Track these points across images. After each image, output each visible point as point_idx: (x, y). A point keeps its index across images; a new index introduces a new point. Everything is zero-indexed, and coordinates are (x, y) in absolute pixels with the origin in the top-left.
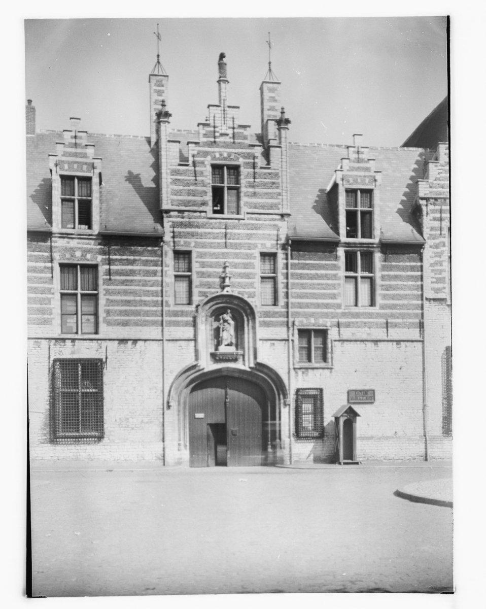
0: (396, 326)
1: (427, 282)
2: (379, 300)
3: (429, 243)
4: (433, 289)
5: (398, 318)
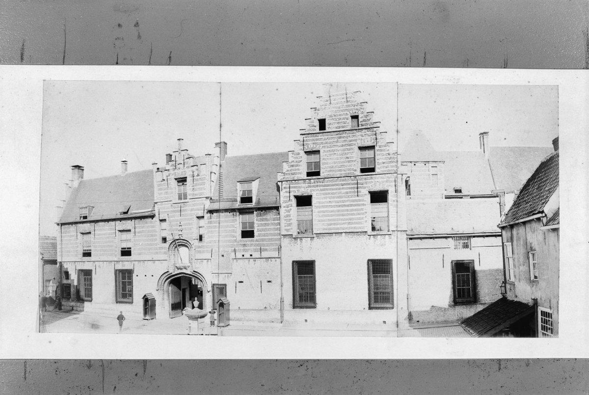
0: (266, 250)
1: (283, 225)
3: (283, 205)
4: (286, 230)
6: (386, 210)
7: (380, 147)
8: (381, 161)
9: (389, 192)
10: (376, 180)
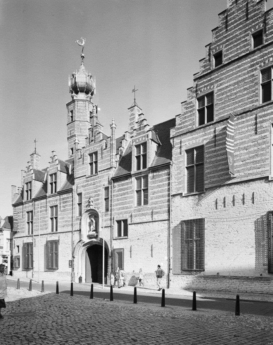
2: (150, 201)
5: (158, 209)
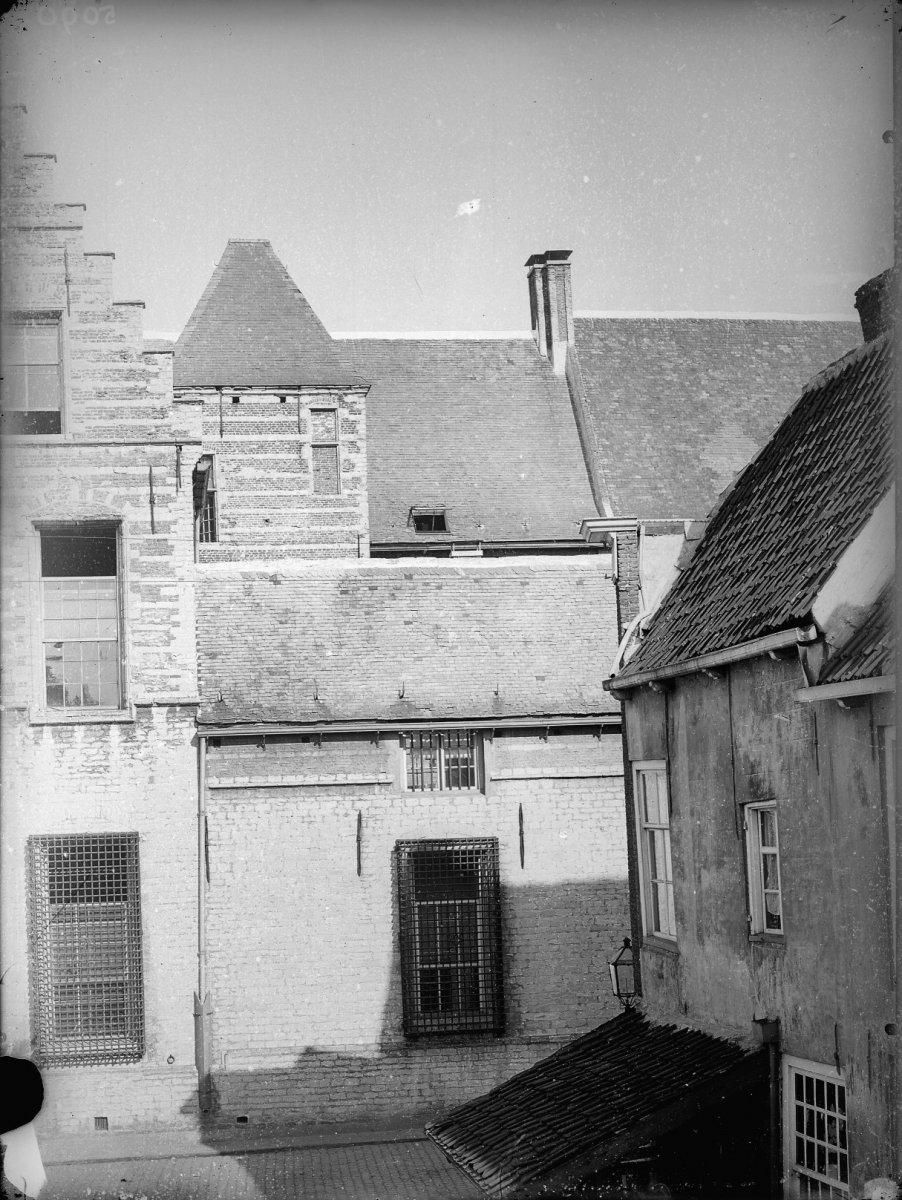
6: (111, 608)
7: (84, 317)
8: (87, 385)
9: (125, 526)
10: (67, 471)
